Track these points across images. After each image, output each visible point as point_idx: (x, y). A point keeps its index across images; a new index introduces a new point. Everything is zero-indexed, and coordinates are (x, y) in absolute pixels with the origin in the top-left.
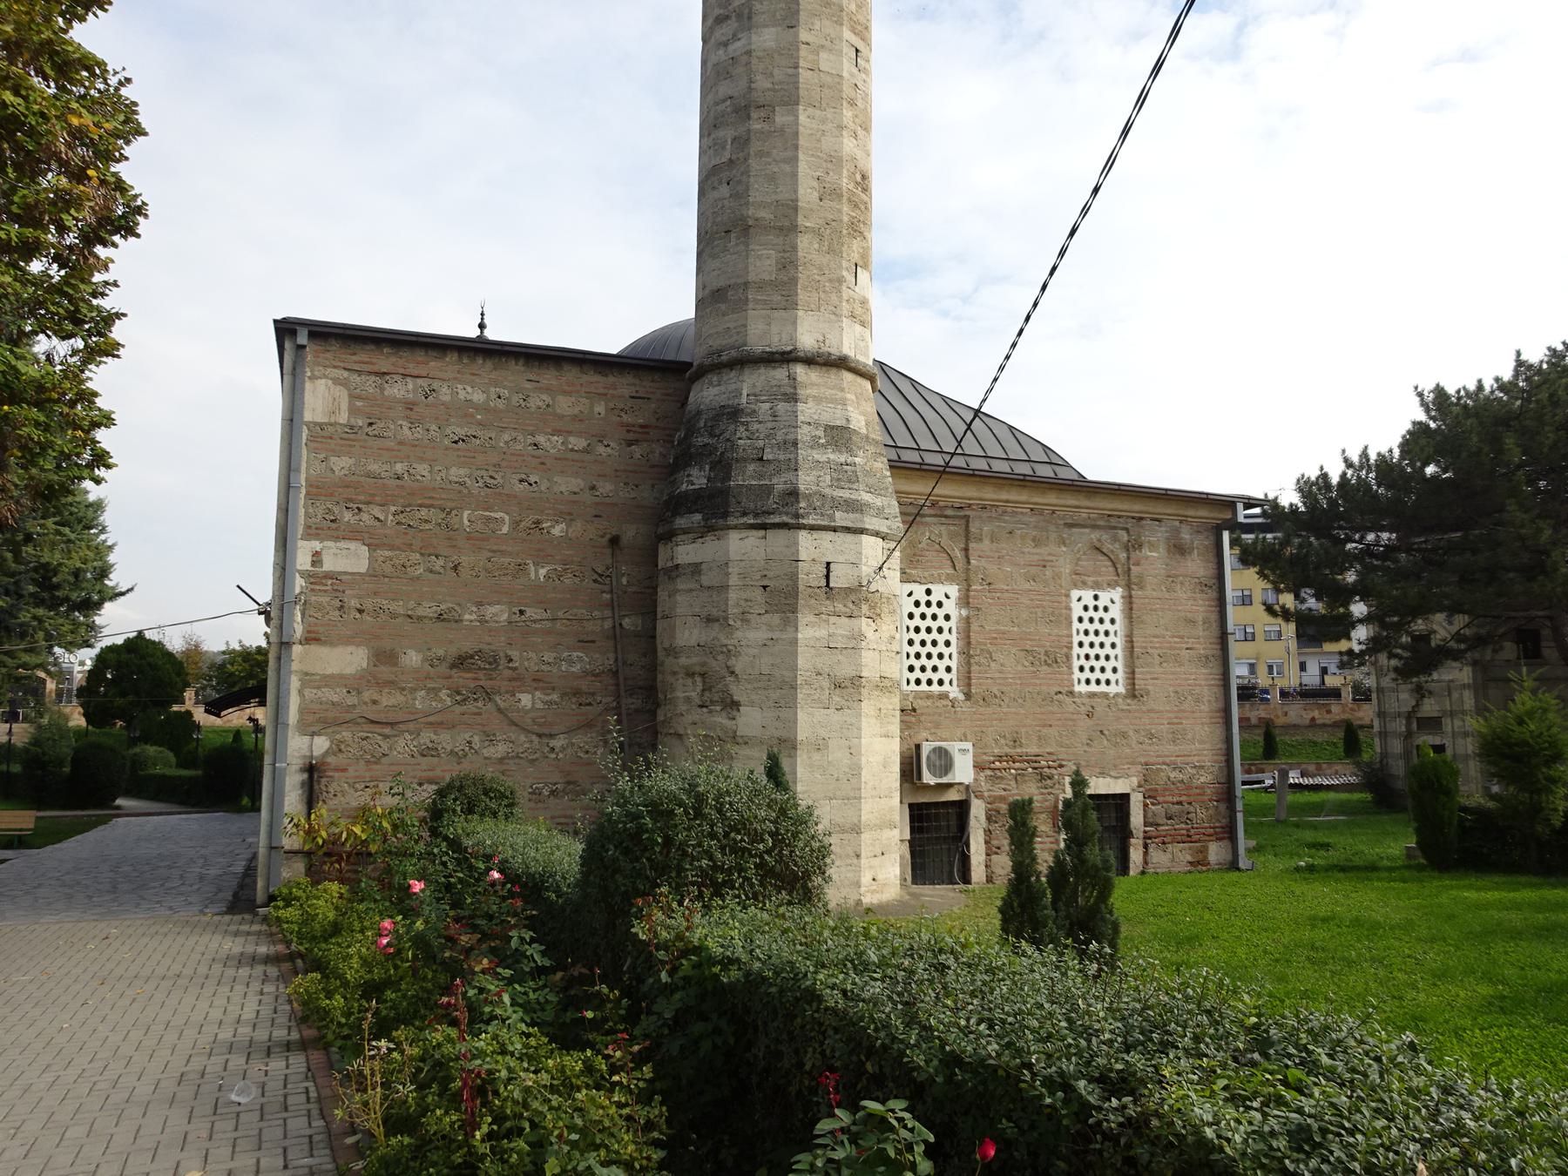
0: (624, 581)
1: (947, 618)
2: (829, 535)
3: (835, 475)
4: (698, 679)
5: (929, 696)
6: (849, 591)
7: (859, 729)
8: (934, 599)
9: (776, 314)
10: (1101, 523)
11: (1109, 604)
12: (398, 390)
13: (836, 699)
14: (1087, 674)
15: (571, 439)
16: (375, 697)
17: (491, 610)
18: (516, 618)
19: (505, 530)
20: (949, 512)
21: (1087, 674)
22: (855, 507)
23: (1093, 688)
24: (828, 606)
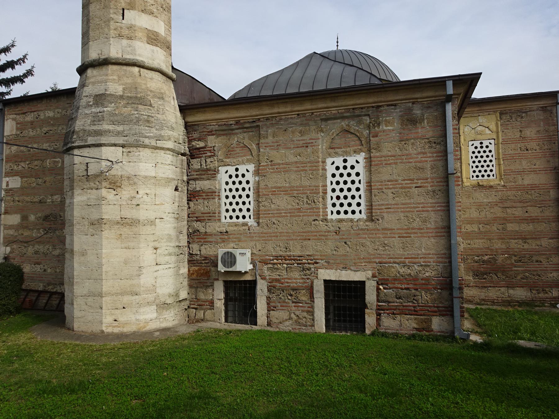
5: (236, 225)
6: (96, 176)
7: (102, 245)
10: (348, 114)
12: (29, 118)
13: (91, 230)
17: (55, 197)
20: (247, 125)
22: (99, 133)
23: (342, 216)
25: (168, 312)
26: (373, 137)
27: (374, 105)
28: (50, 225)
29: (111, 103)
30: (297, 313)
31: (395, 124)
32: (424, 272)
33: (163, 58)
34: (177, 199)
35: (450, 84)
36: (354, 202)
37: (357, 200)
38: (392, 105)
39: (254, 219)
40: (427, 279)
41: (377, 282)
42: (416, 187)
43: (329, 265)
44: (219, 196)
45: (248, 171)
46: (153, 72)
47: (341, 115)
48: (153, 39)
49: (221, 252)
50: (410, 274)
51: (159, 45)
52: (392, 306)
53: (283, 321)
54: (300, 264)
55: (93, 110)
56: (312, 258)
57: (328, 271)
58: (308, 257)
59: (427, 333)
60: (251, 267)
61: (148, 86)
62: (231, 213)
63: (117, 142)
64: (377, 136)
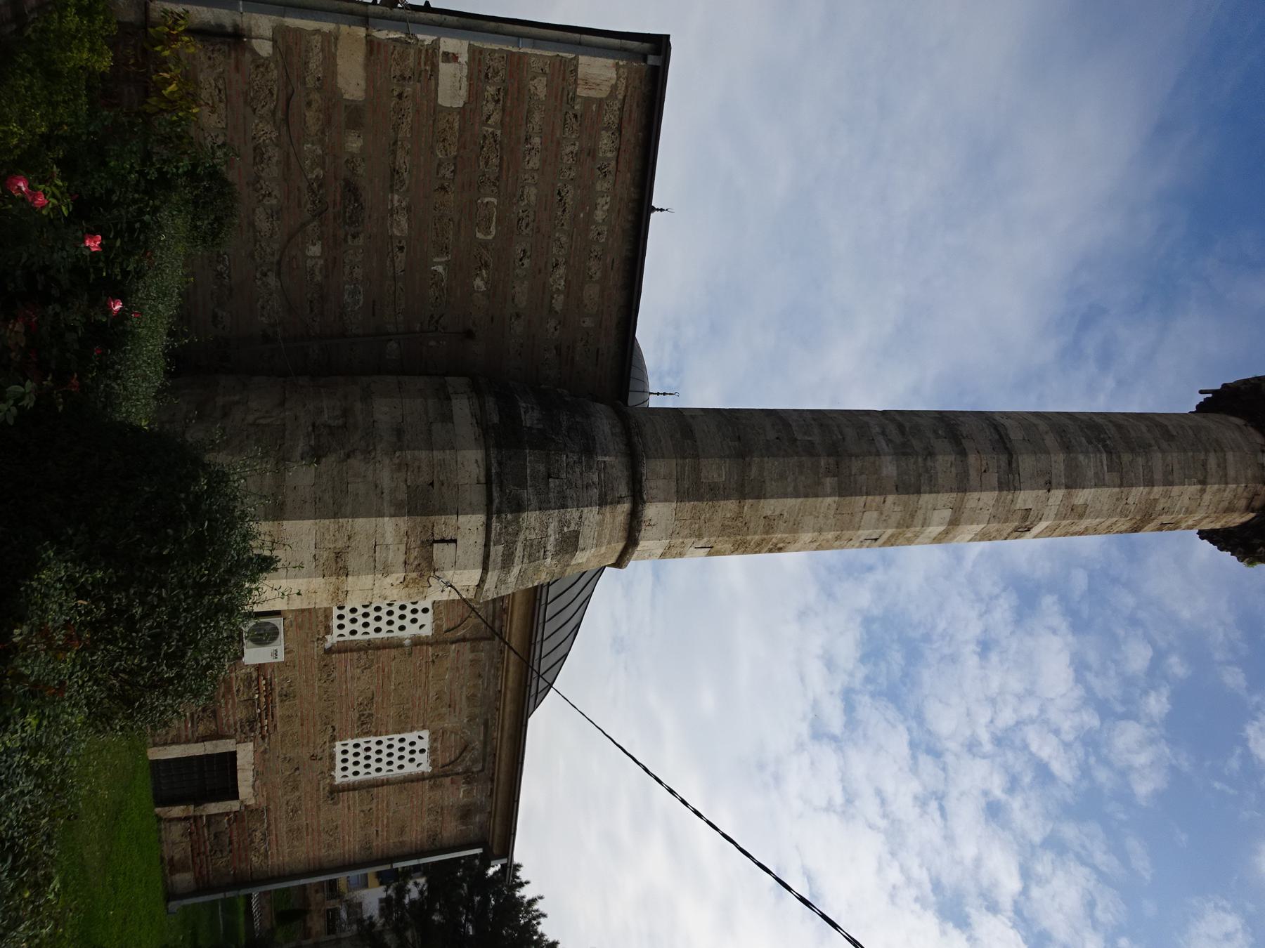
0: (432, 343)
1: (402, 628)
2: (481, 541)
3: (535, 542)
4: (340, 422)
6: (429, 560)
8: (419, 616)
9: (673, 484)
10: (489, 749)
11: (417, 762)
12: (606, 142)
13: (325, 555)
15: (562, 297)
16: (314, 106)
18: (396, 243)
19: (479, 235)
23: (339, 757)
24: (415, 542)
28: (335, 204)
43: (262, 757)
45: (421, 627)
57: (251, 754)
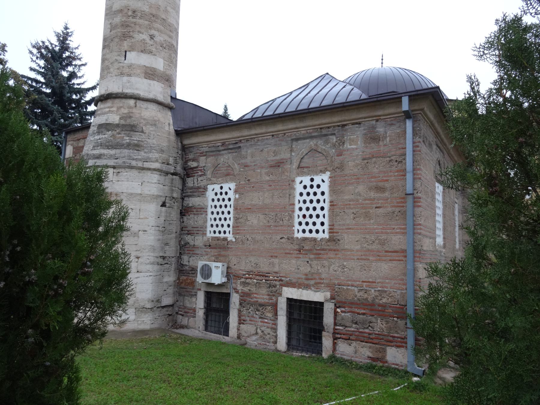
1: (229, 200)
5: (218, 239)
10: (316, 134)
14: (304, 226)
20: (231, 147)
21: (304, 226)
23: (307, 235)
25: (147, 315)
26: (338, 156)
27: (339, 124)
29: (108, 131)
30: (263, 329)
31: (359, 143)
32: (380, 298)
33: (160, 90)
34: (163, 214)
35: (405, 100)
36: (318, 222)
37: (321, 219)
38: (356, 123)
39: (233, 234)
40: (384, 306)
41: (335, 305)
42: (376, 208)
44: (206, 212)
46: (149, 103)
47: (310, 135)
48: (150, 74)
49: (200, 264)
50: (367, 299)
51: (156, 79)
52: (349, 331)
53: (251, 336)
54: (268, 280)
55: (96, 137)
56: (278, 275)
58: (275, 275)
59: (381, 364)
60: (224, 280)
61: (142, 115)
62: (215, 228)
63: (109, 164)
64: (341, 155)
